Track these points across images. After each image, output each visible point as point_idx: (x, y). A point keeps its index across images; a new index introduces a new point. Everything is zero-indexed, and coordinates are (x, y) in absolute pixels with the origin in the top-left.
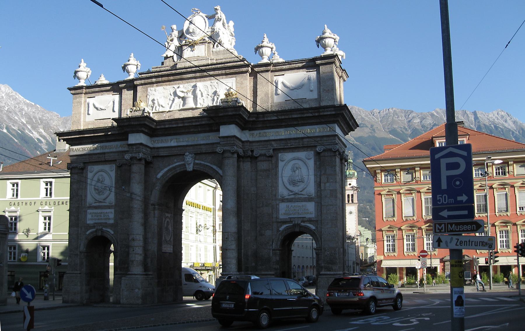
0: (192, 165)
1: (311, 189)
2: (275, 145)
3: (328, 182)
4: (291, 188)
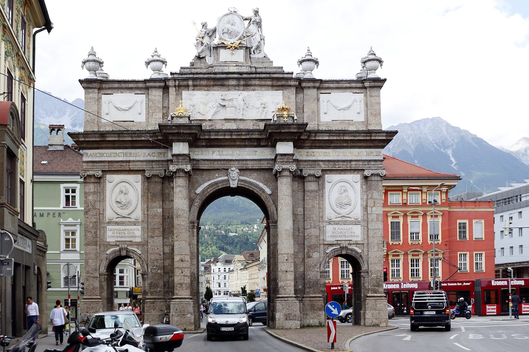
0: (237, 180)
1: (358, 213)
2: (323, 166)
3: (374, 206)
4: (338, 210)
